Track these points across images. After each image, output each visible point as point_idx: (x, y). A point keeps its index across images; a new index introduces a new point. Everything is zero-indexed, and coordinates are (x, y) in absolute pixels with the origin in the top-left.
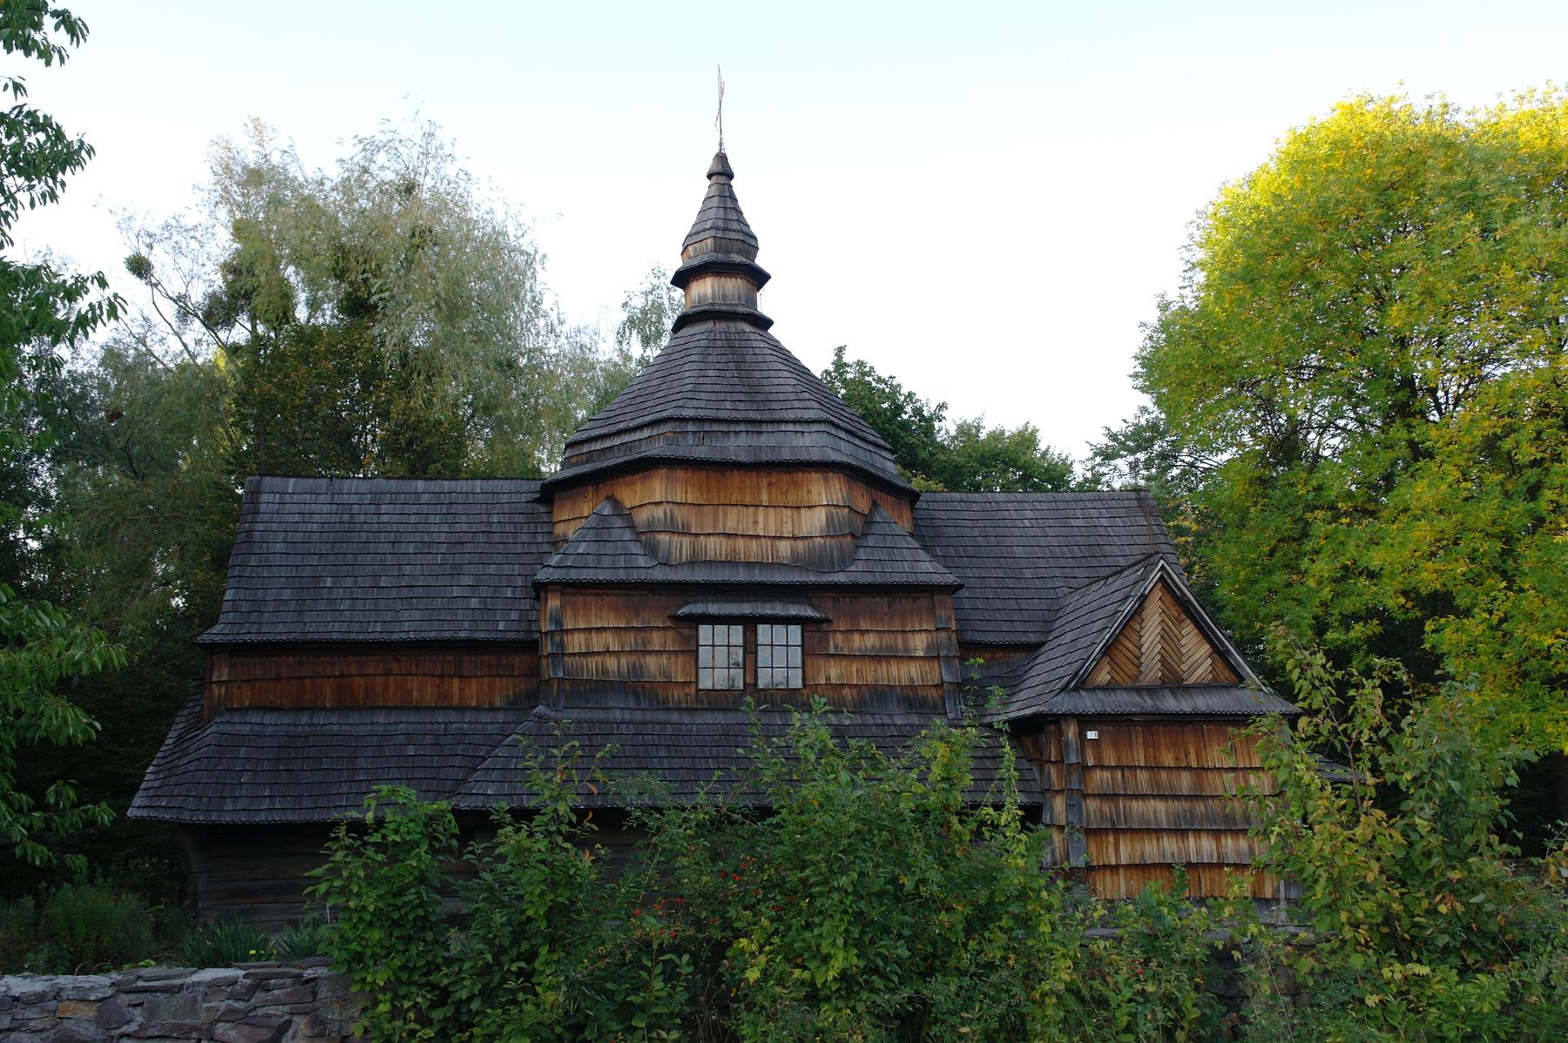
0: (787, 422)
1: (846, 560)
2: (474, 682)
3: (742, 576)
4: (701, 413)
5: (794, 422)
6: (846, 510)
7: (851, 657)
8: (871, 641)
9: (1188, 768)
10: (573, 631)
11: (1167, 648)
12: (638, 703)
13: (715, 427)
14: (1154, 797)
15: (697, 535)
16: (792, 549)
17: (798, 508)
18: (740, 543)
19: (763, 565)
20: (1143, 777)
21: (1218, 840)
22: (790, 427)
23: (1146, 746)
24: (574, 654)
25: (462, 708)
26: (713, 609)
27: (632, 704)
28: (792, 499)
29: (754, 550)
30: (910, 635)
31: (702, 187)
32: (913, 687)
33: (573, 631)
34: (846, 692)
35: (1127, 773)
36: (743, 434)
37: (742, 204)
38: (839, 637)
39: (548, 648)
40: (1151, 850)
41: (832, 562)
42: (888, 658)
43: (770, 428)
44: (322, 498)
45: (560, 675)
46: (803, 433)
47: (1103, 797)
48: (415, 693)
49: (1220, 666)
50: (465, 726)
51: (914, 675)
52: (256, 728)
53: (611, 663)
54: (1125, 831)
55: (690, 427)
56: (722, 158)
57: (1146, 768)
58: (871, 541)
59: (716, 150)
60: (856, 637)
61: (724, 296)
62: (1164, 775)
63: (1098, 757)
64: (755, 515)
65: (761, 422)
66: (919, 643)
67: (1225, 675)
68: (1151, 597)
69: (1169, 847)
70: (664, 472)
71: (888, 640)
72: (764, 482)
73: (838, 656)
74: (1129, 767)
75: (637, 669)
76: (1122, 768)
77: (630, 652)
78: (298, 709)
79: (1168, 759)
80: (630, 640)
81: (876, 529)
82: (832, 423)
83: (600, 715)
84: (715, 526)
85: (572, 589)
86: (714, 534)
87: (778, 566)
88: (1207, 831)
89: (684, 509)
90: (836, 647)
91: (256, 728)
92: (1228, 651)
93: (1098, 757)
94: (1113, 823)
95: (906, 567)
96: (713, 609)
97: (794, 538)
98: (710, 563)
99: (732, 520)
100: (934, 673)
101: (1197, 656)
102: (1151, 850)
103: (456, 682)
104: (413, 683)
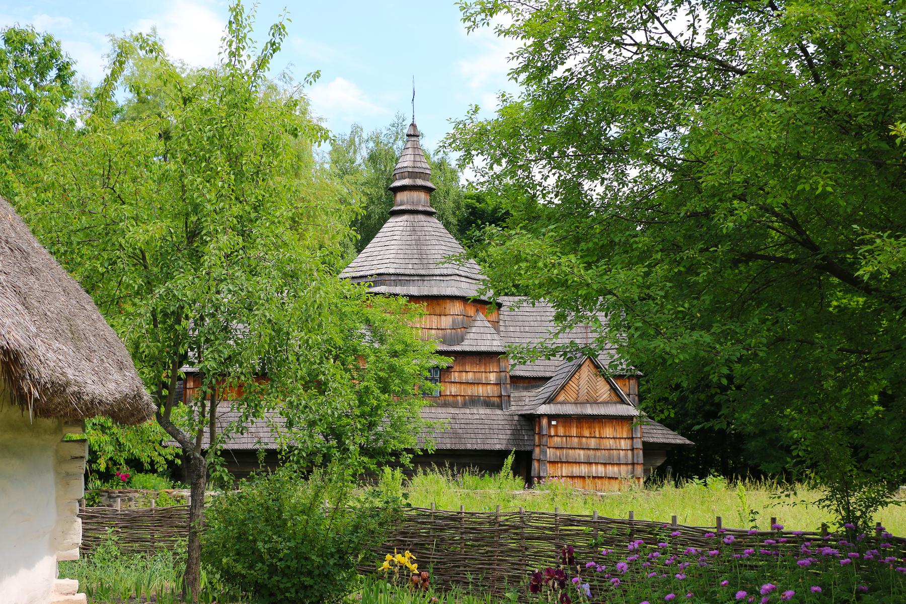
0: (436, 275)
4: (398, 271)
9: (595, 437)
13: (403, 278)
14: (579, 449)
20: (576, 440)
21: (605, 467)
22: (438, 278)
23: (577, 427)
28: (438, 311)
38: (456, 374)
40: (577, 470)
42: (478, 384)
43: (428, 278)
47: (557, 448)
49: (613, 395)
51: (489, 392)
54: (565, 462)
55: (392, 278)
60: (464, 374)
62: (584, 440)
63: (556, 432)
65: (424, 276)
66: (492, 377)
67: (615, 398)
69: (583, 470)
74: (569, 436)
76: (566, 436)
79: (586, 433)
88: (601, 463)
90: (455, 378)
93: (556, 432)
94: (560, 459)
95: (488, 343)
97: (438, 329)
102: (577, 470)
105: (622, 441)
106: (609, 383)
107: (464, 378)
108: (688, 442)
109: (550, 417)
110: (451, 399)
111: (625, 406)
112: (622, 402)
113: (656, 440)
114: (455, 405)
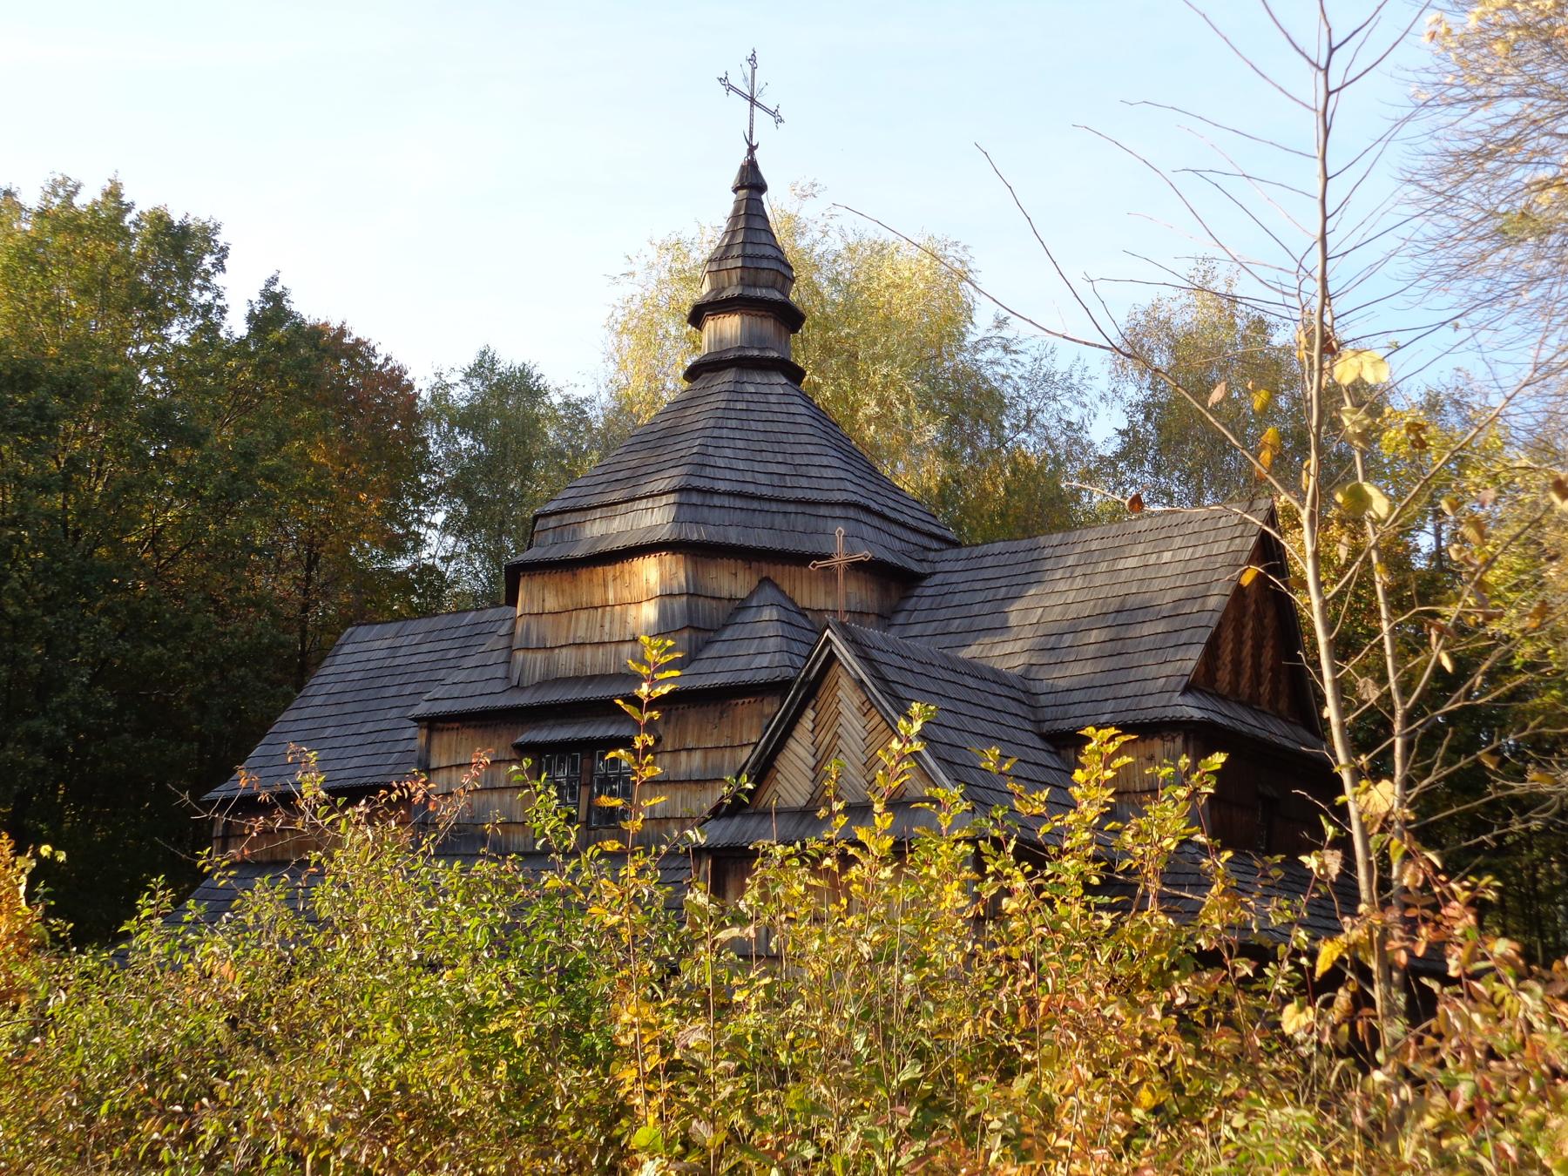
0: (640, 498)
6: (684, 599)
15: (552, 648)
18: (588, 651)
31: (724, 203)
59: (741, 157)
71: (714, 757)
82: (698, 490)
85: (433, 723)
107: (683, 767)
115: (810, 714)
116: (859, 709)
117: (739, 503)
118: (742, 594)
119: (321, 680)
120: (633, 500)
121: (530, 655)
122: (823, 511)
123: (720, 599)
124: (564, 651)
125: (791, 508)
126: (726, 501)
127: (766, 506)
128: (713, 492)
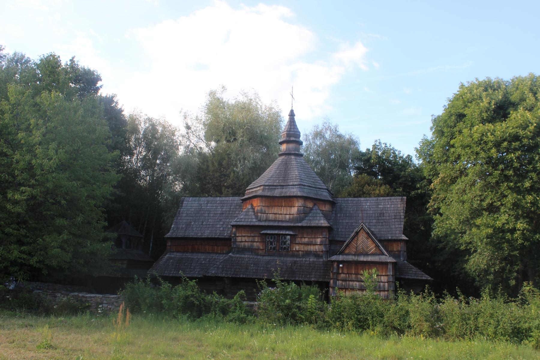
0: (290, 185)
1: (301, 220)
2: (219, 247)
3: (276, 224)
5: (292, 185)
6: (303, 207)
7: (302, 244)
8: (306, 240)
10: (238, 236)
11: (363, 244)
12: (252, 253)
13: (273, 187)
14: (356, 281)
15: (267, 214)
16: (289, 217)
17: (291, 207)
18: (277, 215)
19: (282, 221)
20: (354, 276)
22: (291, 187)
23: (355, 269)
24: (238, 242)
25: (217, 253)
26: (269, 232)
27: (251, 254)
29: (280, 217)
30: (316, 239)
32: (316, 252)
33: (238, 236)
34: (300, 252)
35: (349, 275)
36: (279, 189)
37: (297, 123)
38: (299, 239)
39: (232, 240)
41: (298, 220)
44: (196, 202)
45: (235, 246)
46: (293, 188)
47: (343, 280)
48: (207, 249)
50: (216, 257)
52: (175, 256)
53: (246, 244)
56: (292, 111)
57: (354, 274)
58: (310, 215)
60: (303, 239)
61: (289, 149)
64: (281, 208)
65: (284, 186)
66: (319, 241)
67: (378, 252)
68: (360, 232)
70: (260, 198)
71: (311, 240)
72: (283, 201)
73: (299, 244)
75: (252, 245)
77: (251, 242)
78: (184, 252)
80: (251, 239)
81: (312, 212)
82: (302, 185)
83: (243, 256)
84: (272, 212)
85: (237, 227)
86: (271, 213)
87: (286, 221)
89: (265, 207)
90: (298, 241)
91: (175, 256)
92: (379, 246)
93: (342, 271)
94: (345, 287)
96: (269, 232)
97: (290, 214)
98: (270, 221)
99: (275, 210)
100: (323, 248)
101: (371, 247)
103: (216, 247)
104: (207, 247)
105: (382, 277)
106: (375, 243)
107: (303, 241)
108: (429, 278)
109: (339, 262)
110: (296, 253)
111: (384, 256)
112: (383, 254)
113: (410, 277)
114: (297, 256)
115: (356, 237)
116: (367, 237)
117: (309, 188)
118: (311, 207)
119: (182, 210)
120: (288, 185)
121: (262, 214)
122: (322, 190)
123: (307, 207)
124: (271, 214)
125: (317, 189)
126: (307, 187)
127: (314, 189)
128: (305, 185)
